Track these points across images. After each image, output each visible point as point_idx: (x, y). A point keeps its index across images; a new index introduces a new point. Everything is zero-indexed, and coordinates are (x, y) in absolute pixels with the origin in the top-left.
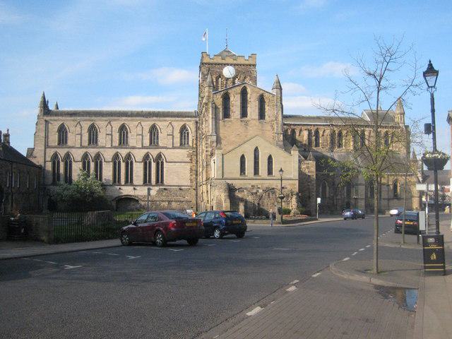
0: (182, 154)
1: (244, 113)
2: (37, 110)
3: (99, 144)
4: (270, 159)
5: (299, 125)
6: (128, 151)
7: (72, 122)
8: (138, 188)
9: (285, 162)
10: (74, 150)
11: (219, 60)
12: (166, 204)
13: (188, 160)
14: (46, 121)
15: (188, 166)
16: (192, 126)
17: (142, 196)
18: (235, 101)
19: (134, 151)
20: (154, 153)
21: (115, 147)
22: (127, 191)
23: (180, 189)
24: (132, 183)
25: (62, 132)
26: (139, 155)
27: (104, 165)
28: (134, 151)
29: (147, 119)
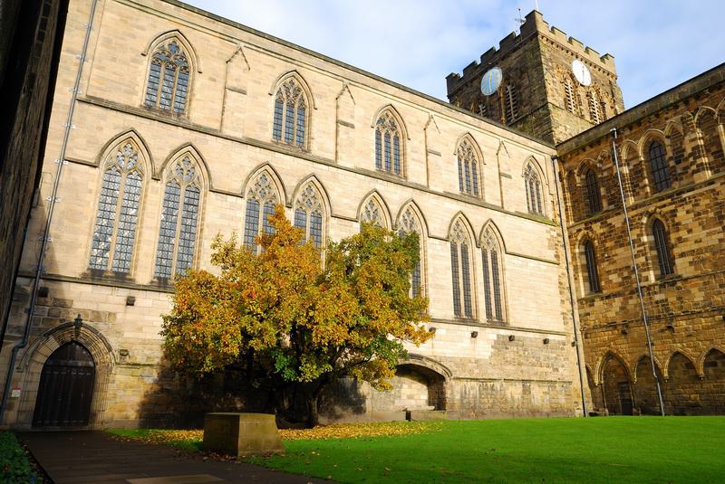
7: (215, 41)
13: (550, 255)
17: (451, 359)
23: (546, 342)
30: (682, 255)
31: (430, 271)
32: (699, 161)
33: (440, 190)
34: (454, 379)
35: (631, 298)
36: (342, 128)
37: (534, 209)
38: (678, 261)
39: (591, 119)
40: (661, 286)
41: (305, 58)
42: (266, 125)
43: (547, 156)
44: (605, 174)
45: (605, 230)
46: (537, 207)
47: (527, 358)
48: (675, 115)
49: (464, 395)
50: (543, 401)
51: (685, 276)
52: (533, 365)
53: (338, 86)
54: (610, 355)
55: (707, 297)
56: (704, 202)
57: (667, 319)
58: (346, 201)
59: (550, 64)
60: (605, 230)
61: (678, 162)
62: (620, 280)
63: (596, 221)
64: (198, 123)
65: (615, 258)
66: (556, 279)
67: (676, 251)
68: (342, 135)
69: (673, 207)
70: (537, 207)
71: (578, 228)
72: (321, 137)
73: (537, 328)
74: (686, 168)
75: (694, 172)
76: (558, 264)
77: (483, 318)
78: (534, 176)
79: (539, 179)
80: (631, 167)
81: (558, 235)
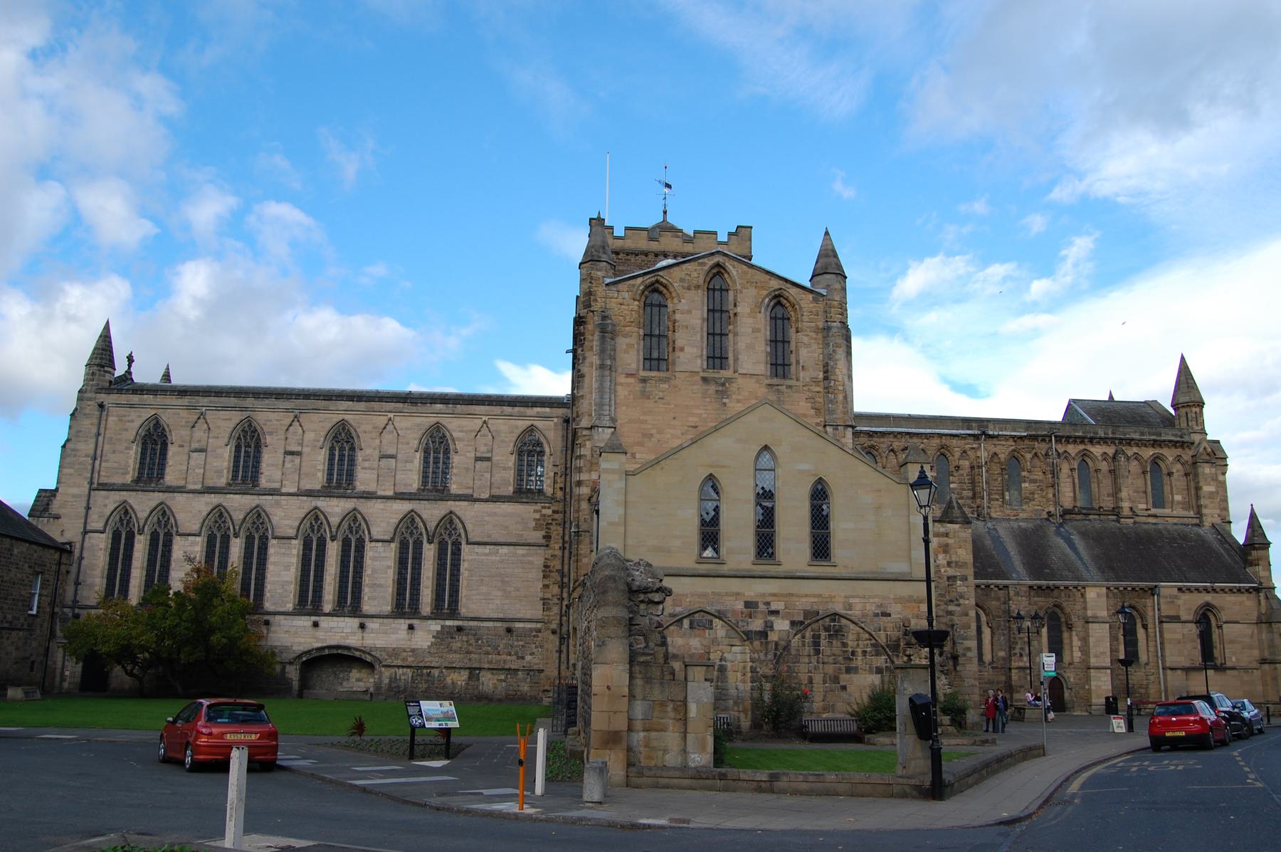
0: (520, 518)
1: (717, 358)
2: (77, 378)
3: (264, 482)
4: (820, 494)
5: (883, 434)
6: (348, 505)
7: (184, 413)
8: (372, 625)
9: (878, 508)
10: (180, 498)
11: (643, 244)
12: (460, 678)
13: (538, 536)
14: (101, 406)
16: (551, 435)
17: (383, 649)
18: (689, 312)
19: (372, 510)
20: (432, 513)
21: (310, 494)
22: (340, 631)
23: (509, 630)
24: (356, 611)
25: (154, 443)
27: (274, 548)
29: (414, 409)
33: (390, 493)
36: (289, 457)
42: (221, 471)
47: (480, 647)
49: (393, 679)
50: (496, 688)
52: (487, 653)
58: (286, 522)
64: (169, 484)
68: (288, 465)
72: (271, 469)
73: (501, 616)
81: (554, 512)
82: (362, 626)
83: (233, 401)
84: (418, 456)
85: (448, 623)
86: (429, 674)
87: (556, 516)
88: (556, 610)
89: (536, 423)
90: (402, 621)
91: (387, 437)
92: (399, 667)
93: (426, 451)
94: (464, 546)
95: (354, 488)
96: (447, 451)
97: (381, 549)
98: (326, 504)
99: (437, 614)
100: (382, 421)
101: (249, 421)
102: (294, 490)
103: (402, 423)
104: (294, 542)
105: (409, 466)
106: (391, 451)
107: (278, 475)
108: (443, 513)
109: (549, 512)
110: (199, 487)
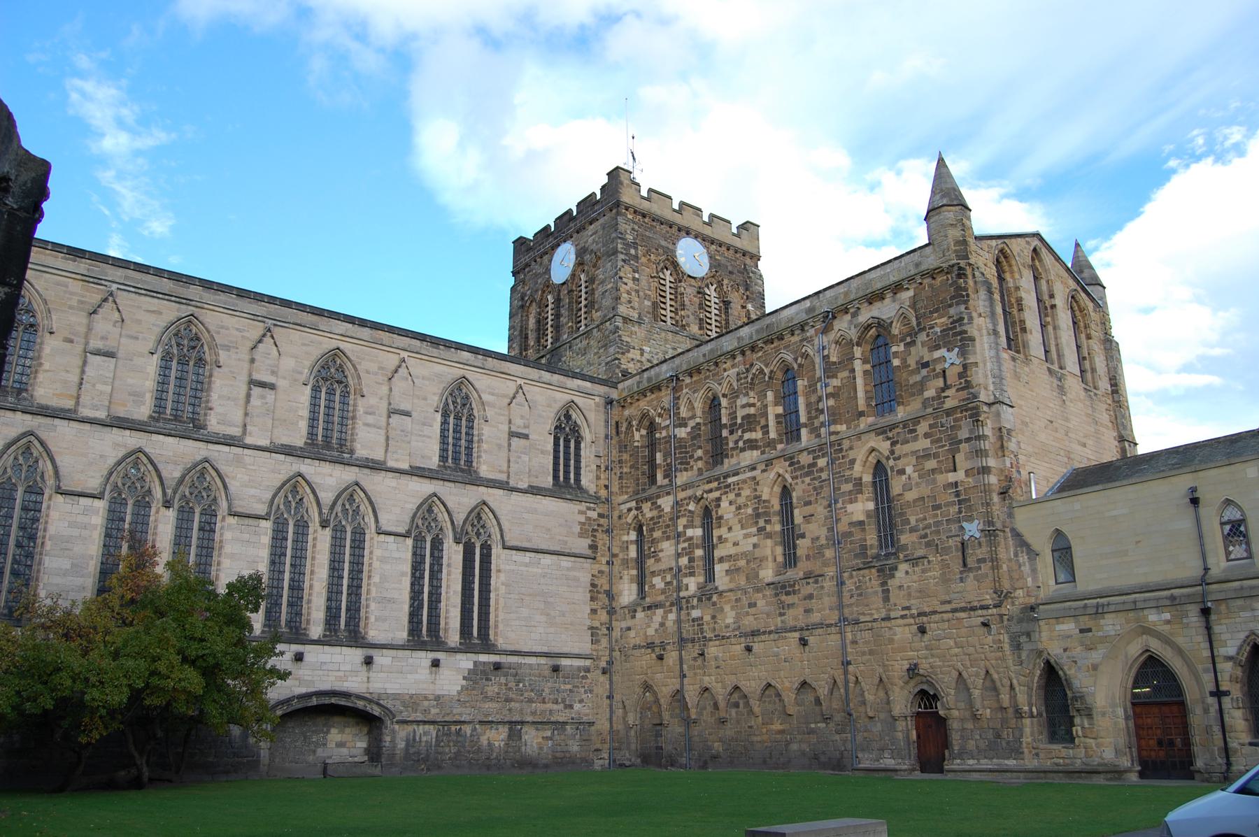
0: (559, 519)
6: (347, 475)
7: (76, 286)
8: (382, 658)
12: (496, 737)
13: (582, 545)
15: (584, 573)
16: (591, 416)
17: (396, 697)
21: (288, 451)
23: (556, 669)
24: (355, 638)
26: (397, 500)
28: (378, 484)
29: (435, 352)
30: (721, 560)
31: (376, 579)
32: (747, 436)
33: (405, 466)
34: (398, 722)
35: (671, 611)
36: (256, 391)
37: (567, 478)
38: (718, 568)
39: (701, 328)
40: (700, 600)
41: (208, 296)
42: (143, 395)
43: (597, 399)
44: (664, 433)
45: (655, 513)
46: (572, 476)
47: (521, 692)
48: (733, 366)
49: (411, 742)
50: (541, 748)
51: (720, 589)
52: (531, 701)
53: (257, 330)
54: (647, 687)
55: (738, 618)
56: (746, 492)
57: (691, 640)
58: (253, 491)
59: (633, 251)
60: (655, 513)
61: (731, 433)
62: (662, 585)
63: (647, 500)
64: (43, 402)
65: (661, 554)
66: (586, 578)
67: (718, 553)
68: (255, 401)
69: (716, 494)
70: (572, 476)
71: (628, 505)
72: (224, 405)
73: (545, 649)
74: (736, 442)
75: (743, 450)
76: (594, 558)
77: (454, 638)
78: (575, 430)
79: (582, 434)
80: (689, 429)
81: (600, 515)
82: (368, 661)
83: (166, 285)
84: (438, 417)
85: (483, 658)
86: (458, 733)
87: (602, 521)
88: (604, 642)
89: (576, 399)
90: (422, 654)
91: (400, 384)
92: (418, 722)
93: (445, 415)
94: (496, 551)
95: (352, 452)
96: (471, 419)
97: (393, 546)
98: (314, 470)
99: (467, 646)
100: (392, 360)
101: (191, 319)
102: (264, 442)
103: (419, 367)
104: (263, 523)
105: (427, 430)
106: (404, 406)
107: (238, 416)
108: (473, 502)
109: (594, 515)
110: (101, 414)
